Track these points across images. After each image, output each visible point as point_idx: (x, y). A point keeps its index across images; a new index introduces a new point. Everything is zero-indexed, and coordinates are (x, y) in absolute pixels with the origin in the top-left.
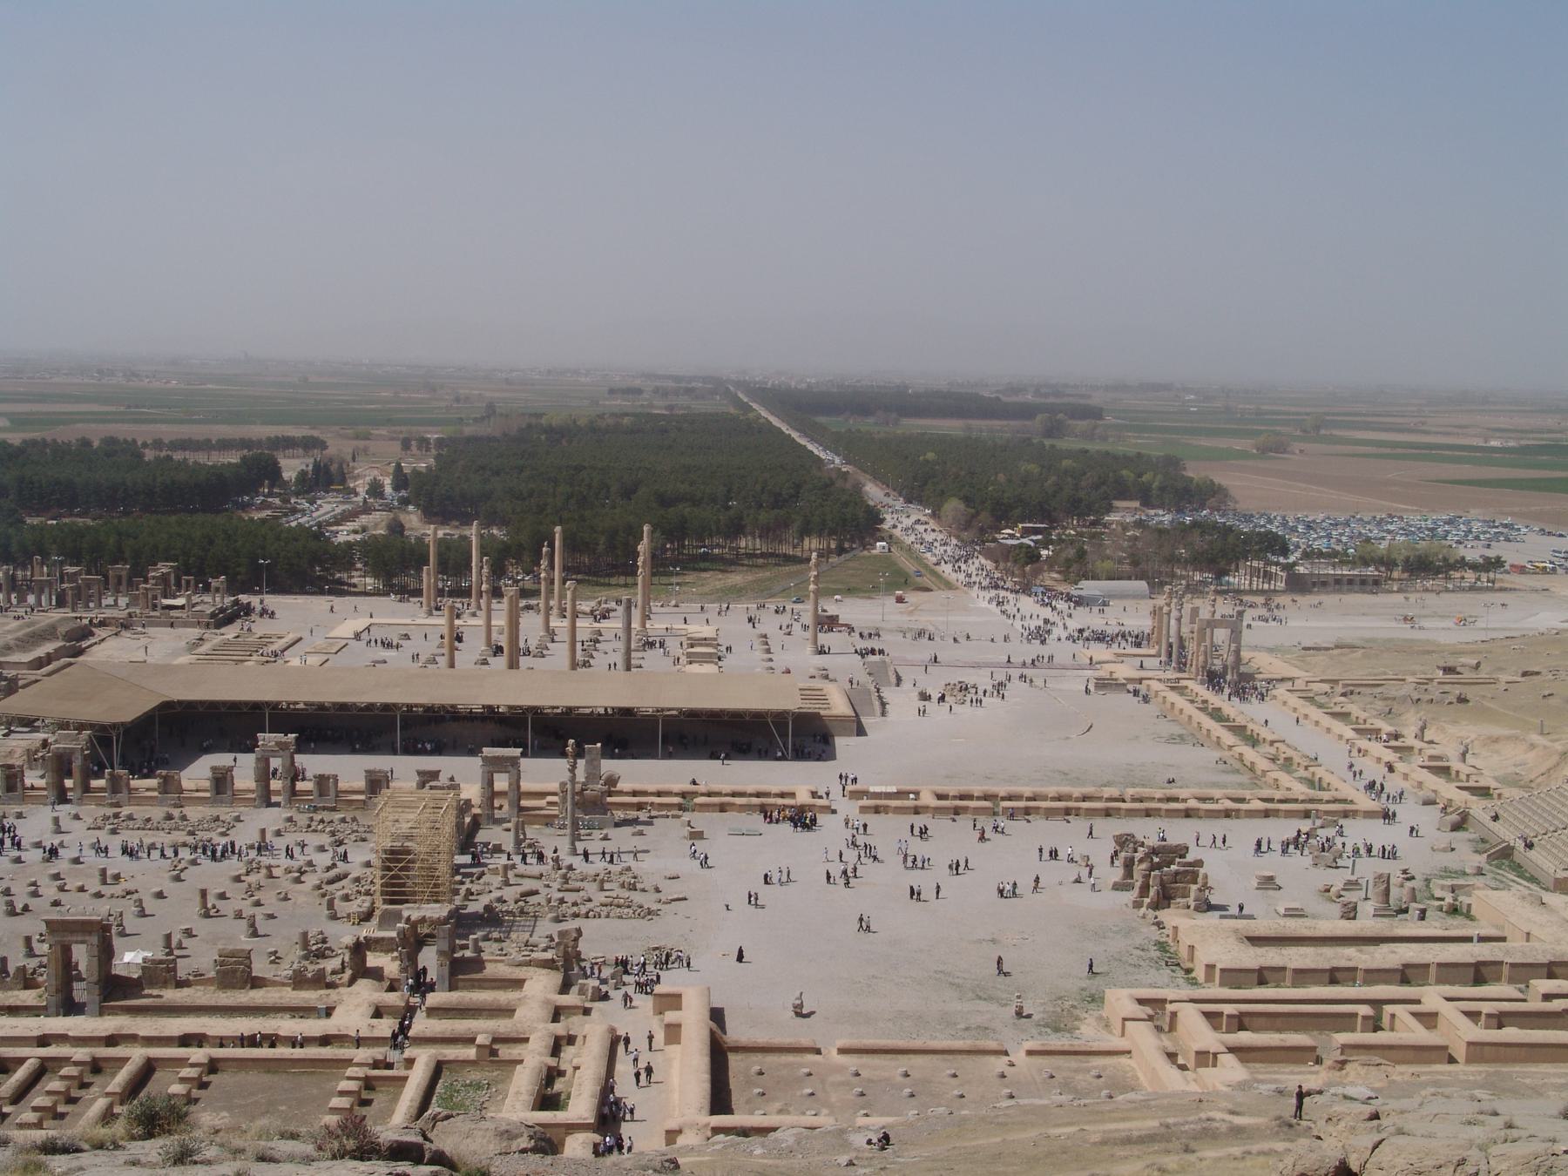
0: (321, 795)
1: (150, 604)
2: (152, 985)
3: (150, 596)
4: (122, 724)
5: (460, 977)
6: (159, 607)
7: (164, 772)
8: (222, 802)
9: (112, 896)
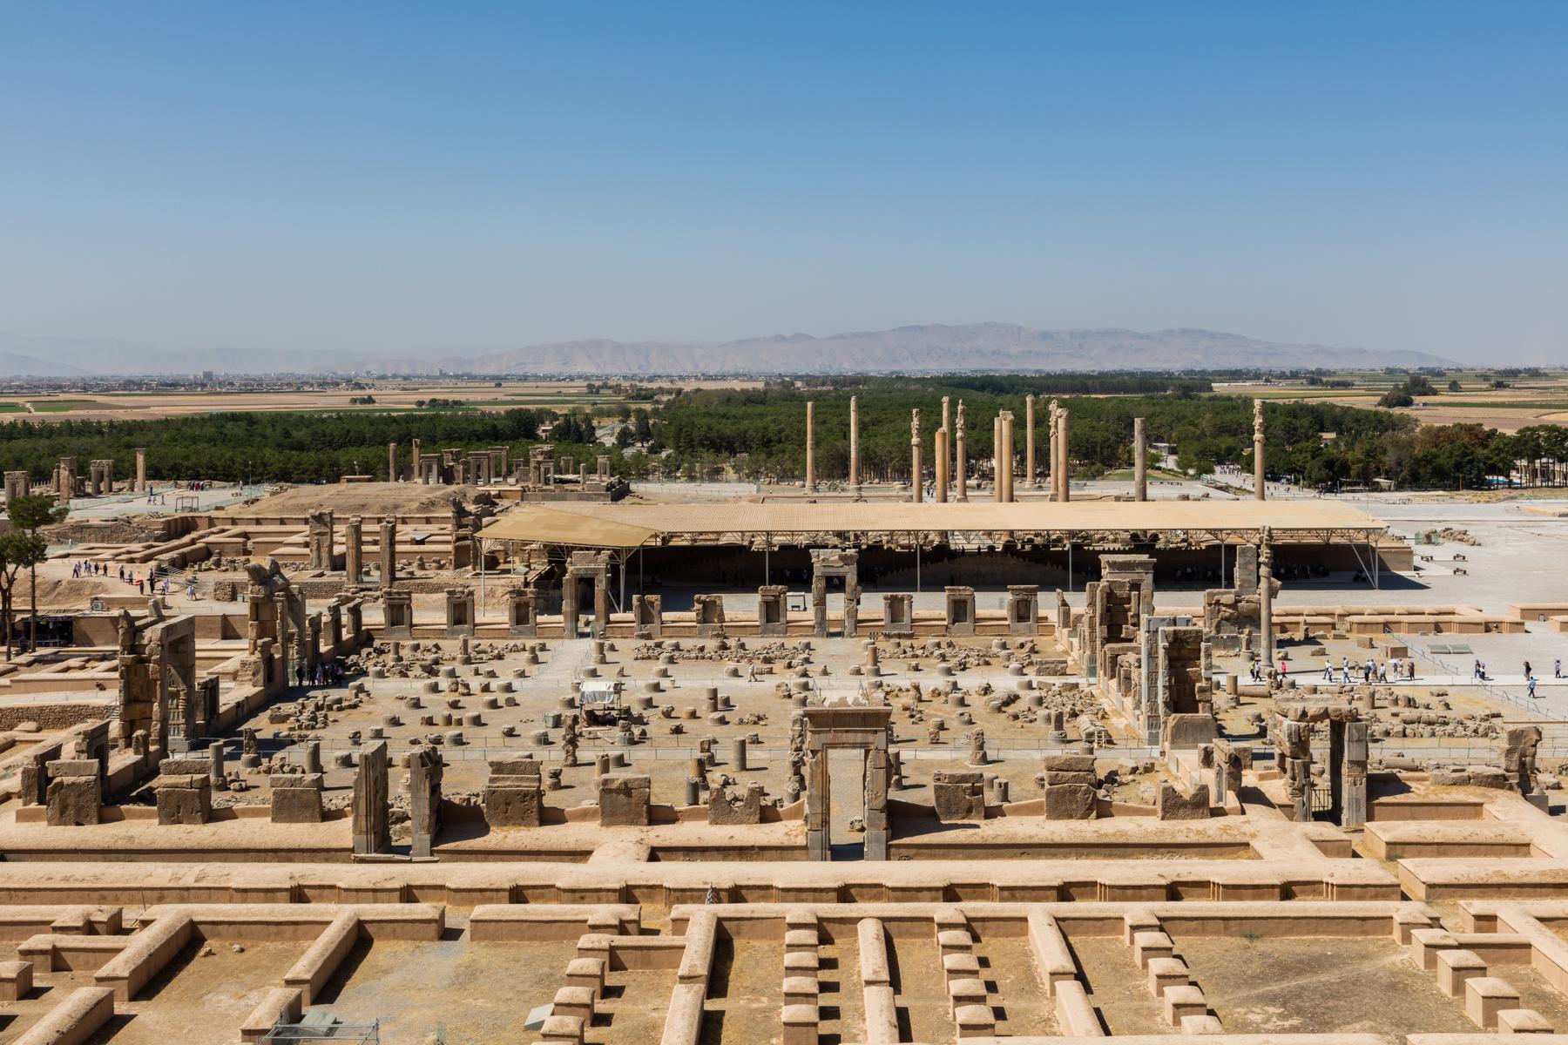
0: (893, 621)
1: (542, 479)
2: (949, 815)
3: (542, 470)
4: (629, 549)
5: (1383, 799)
6: (552, 481)
7: (703, 597)
8: (773, 632)
9: (741, 722)
